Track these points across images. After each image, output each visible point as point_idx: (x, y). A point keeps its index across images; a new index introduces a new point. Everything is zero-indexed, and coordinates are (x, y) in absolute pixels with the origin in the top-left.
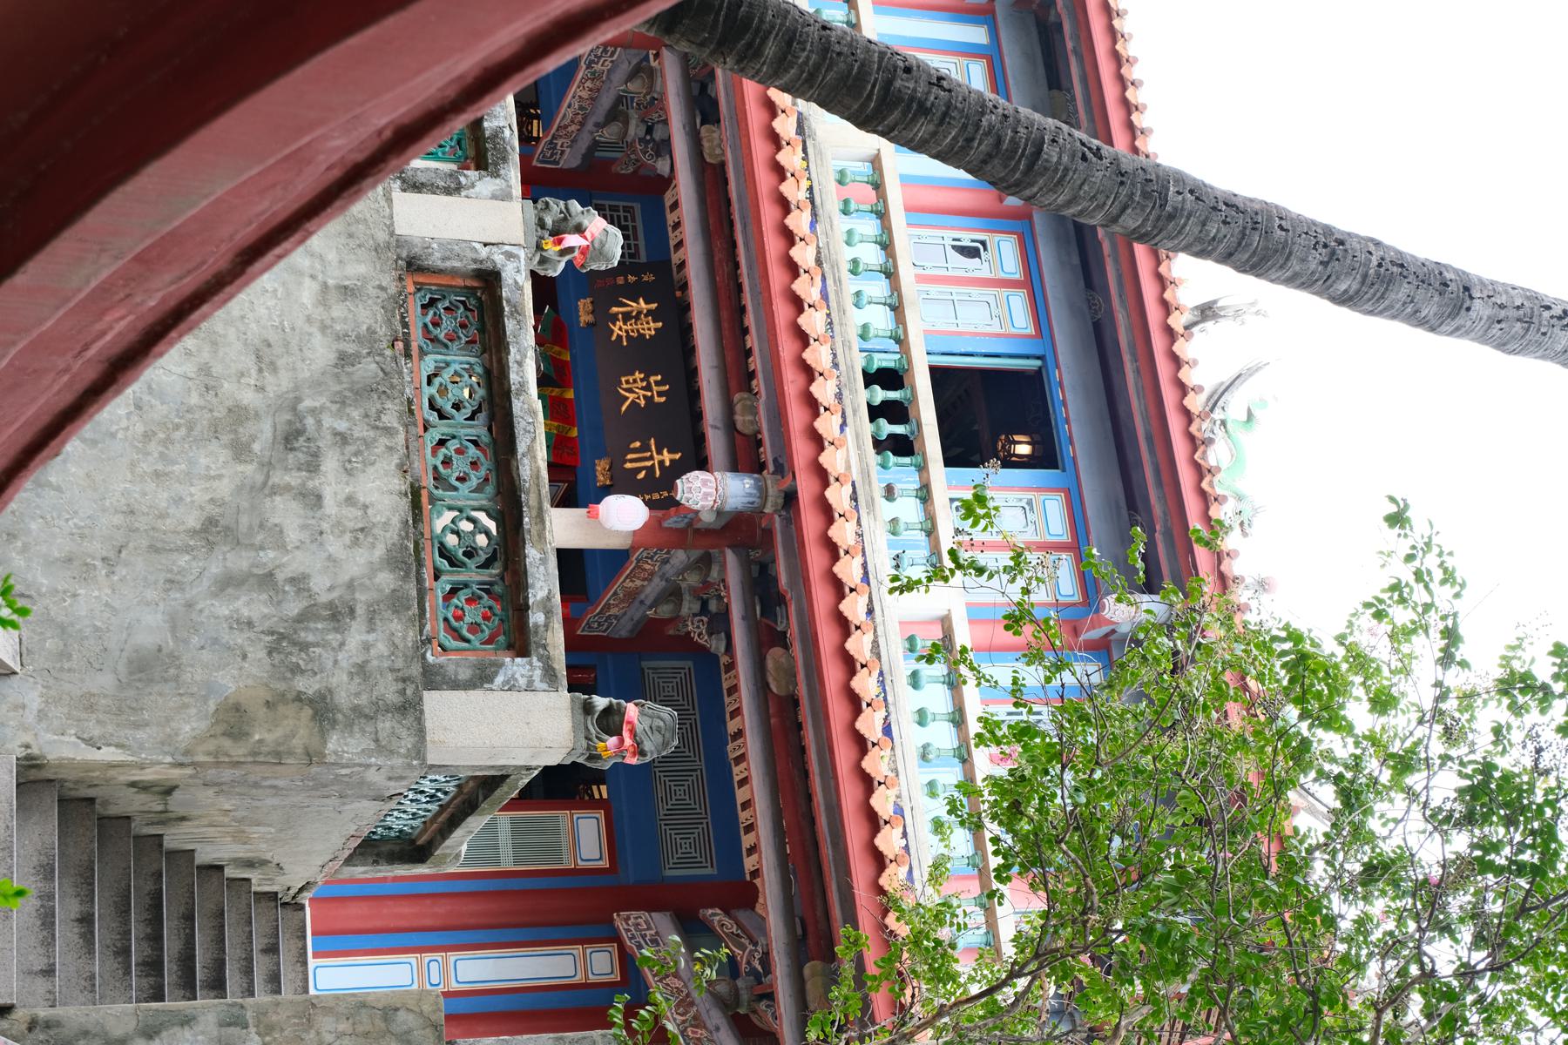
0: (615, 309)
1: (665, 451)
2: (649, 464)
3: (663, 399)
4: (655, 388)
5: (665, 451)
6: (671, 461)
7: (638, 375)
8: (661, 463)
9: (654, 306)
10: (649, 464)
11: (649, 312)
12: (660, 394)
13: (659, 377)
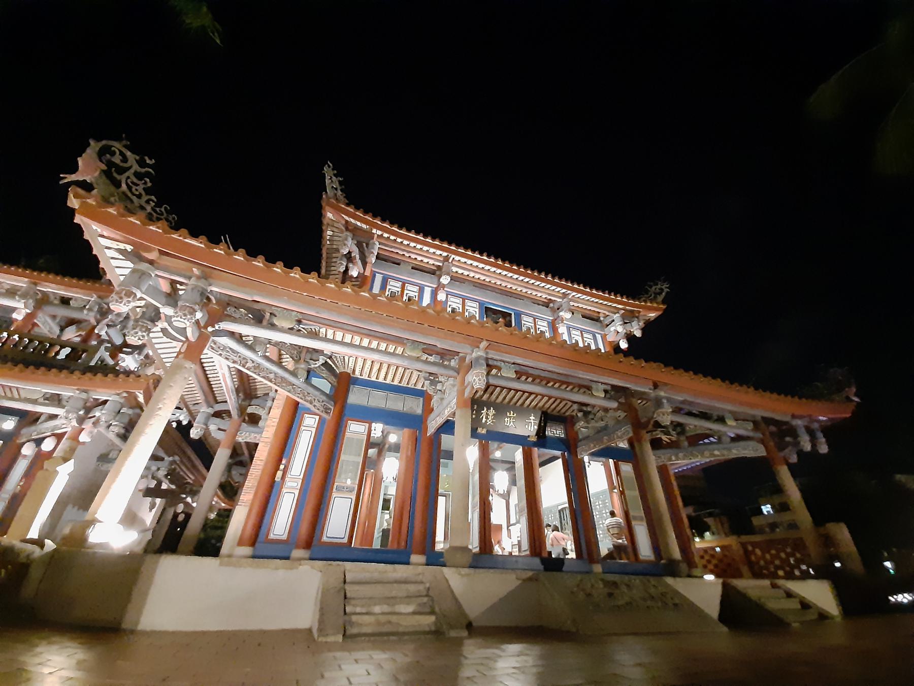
0: (484, 421)
1: (530, 418)
2: (533, 424)
3: (515, 414)
4: (512, 415)
5: (530, 418)
6: (534, 416)
7: (506, 419)
8: (533, 420)
9: (485, 409)
10: (533, 424)
11: (487, 410)
12: (514, 415)
13: (508, 413)
